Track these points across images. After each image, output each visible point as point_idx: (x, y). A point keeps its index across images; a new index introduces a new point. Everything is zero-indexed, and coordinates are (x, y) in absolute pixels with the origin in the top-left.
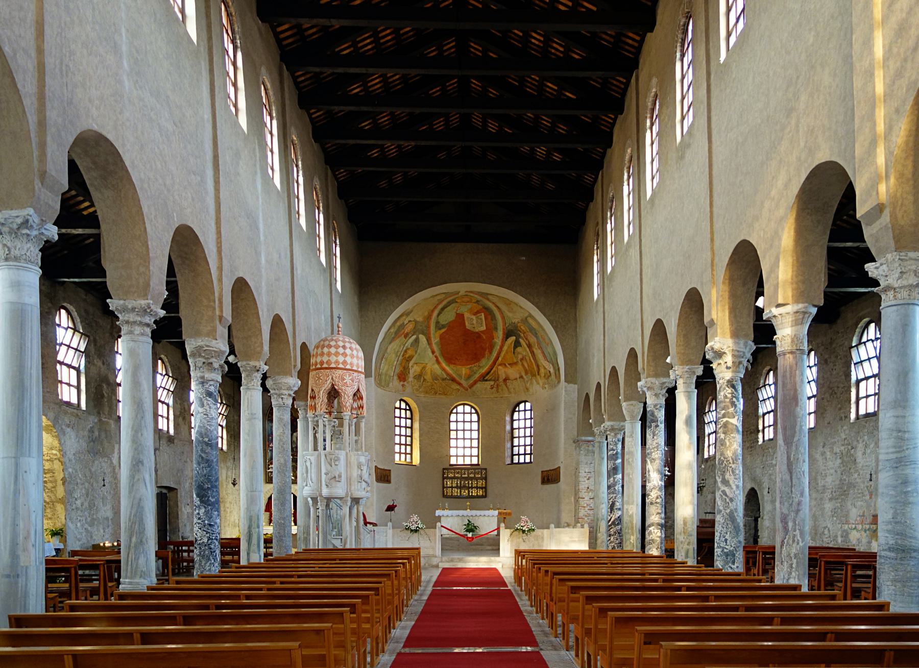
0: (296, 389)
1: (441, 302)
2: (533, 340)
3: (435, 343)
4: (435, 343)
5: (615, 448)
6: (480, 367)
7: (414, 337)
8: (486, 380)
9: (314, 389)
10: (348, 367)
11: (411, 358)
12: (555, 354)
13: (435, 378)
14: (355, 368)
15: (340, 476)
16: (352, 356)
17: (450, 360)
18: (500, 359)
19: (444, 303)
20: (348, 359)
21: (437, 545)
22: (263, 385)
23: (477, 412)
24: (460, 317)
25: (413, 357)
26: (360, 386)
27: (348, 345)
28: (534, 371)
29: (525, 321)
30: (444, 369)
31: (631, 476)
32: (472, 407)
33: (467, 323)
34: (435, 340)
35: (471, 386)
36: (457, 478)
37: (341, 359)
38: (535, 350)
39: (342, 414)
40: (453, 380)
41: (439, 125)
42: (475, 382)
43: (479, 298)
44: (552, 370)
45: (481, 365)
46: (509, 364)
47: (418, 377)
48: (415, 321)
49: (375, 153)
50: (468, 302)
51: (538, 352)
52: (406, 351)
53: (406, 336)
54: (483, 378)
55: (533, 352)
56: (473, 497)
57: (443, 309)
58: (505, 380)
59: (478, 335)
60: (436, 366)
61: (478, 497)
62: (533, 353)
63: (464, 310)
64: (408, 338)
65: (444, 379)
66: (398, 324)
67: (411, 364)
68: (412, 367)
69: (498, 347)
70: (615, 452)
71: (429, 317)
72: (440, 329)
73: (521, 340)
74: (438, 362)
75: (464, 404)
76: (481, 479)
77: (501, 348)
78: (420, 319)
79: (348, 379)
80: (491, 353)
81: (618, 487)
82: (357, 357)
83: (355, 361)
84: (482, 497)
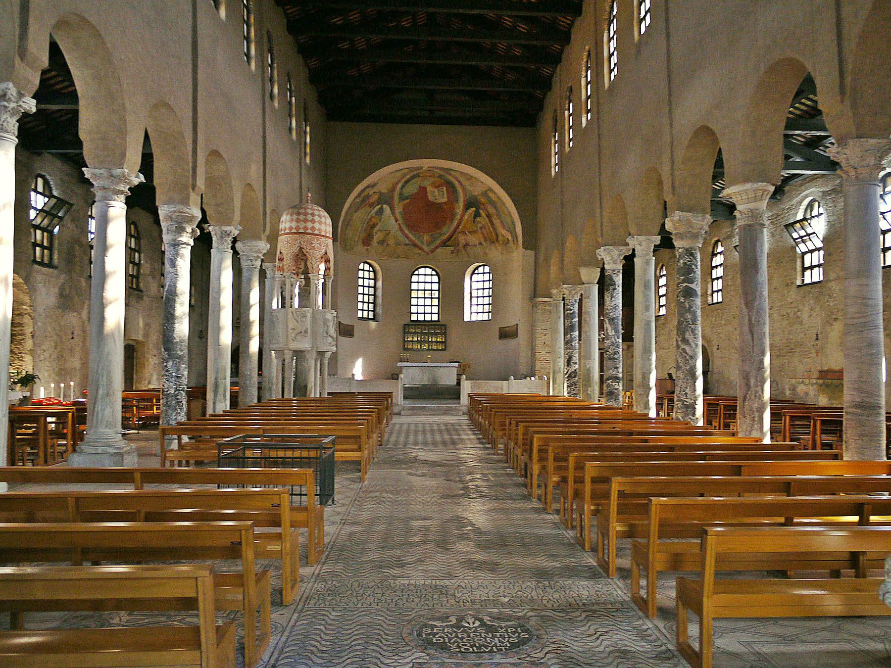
0: (265, 251)
1: (404, 176)
2: (492, 210)
3: (399, 213)
4: (399, 213)
5: (572, 308)
6: (441, 235)
7: (379, 207)
8: (447, 246)
9: (282, 251)
10: (316, 232)
11: (374, 225)
12: (513, 223)
13: (398, 244)
14: (323, 233)
15: (306, 332)
16: (320, 223)
17: (411, 228)
18: (460, 227)
19: (408, 177)
20: (317, 225)
21: (399, 396)
22: (233, 248)
23: (437, 274)
24: (423, 189)
25: (377, 224)
26: (328, 250)
27: (316, 212)
28: (494, 239)
29: (485, 194)
30: (407, 236)
31: (588, 334)
32: (433, 269)
33: (429, 197)
34: (398, 210)
35: (433, 251)
36: (418, 333)
37: (309, 225)
38: (494, 220)
39: (309, 275)
40: (415, 245)
41: (406, 23)
42: (437, 248)
43: (442, 173)
44: (510, 238)
45: (442, 232)
46: (469, 232)
47: (381, 242)
48: (380, 192)
49: (345, 45)
50: (431, 176)
51: (496, 222)
52: (370, 219)
53: (372, 205)
54: (444, 244)
55: (492, 221)
56: (432, 349)
57: (406, 182)
58: (465, 246)
59: (440, 205)
60: (399, 233)
61: (437, 350)
62: (492, 223)
63: (426, 183)
64: (372, 207)
65: (406, 245)
66: (363, 195)
67: (376, 230)
68: (376, 233)
69: (459, 217)
70: (572, 312)
71: (392, 190)
72: (404, 200)
73: (481, 211)
74: (401, 230)
75: (425, 267)
76: (441, 334)
77: (462, 218)
78: (384, 191)
79: (316, 244)
80: (452, 220)
81: (576, 343)
82: (325, 223)
83: (323, 227)
84: (442, 350)
